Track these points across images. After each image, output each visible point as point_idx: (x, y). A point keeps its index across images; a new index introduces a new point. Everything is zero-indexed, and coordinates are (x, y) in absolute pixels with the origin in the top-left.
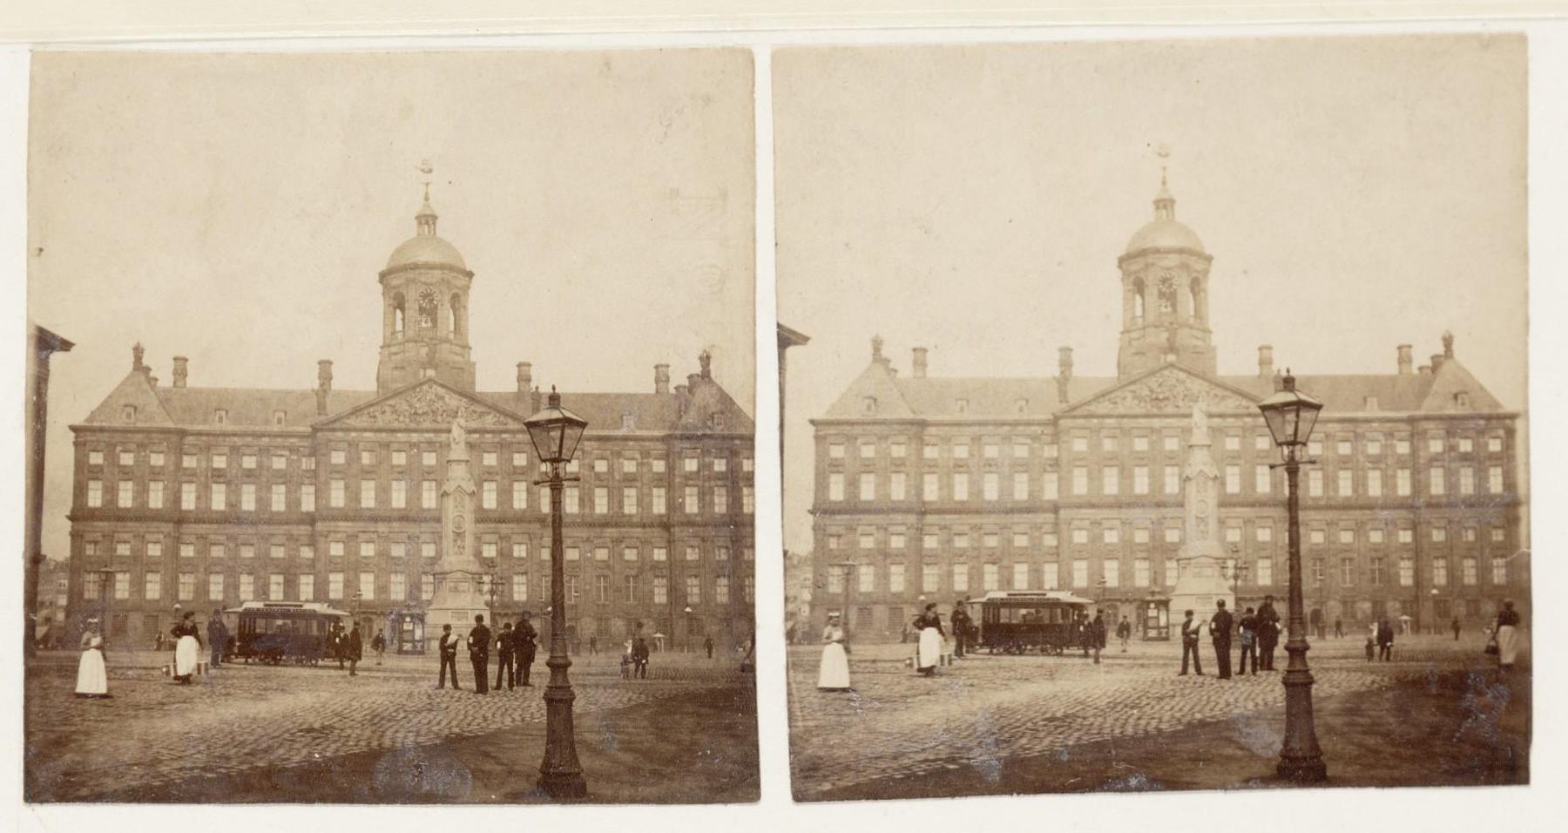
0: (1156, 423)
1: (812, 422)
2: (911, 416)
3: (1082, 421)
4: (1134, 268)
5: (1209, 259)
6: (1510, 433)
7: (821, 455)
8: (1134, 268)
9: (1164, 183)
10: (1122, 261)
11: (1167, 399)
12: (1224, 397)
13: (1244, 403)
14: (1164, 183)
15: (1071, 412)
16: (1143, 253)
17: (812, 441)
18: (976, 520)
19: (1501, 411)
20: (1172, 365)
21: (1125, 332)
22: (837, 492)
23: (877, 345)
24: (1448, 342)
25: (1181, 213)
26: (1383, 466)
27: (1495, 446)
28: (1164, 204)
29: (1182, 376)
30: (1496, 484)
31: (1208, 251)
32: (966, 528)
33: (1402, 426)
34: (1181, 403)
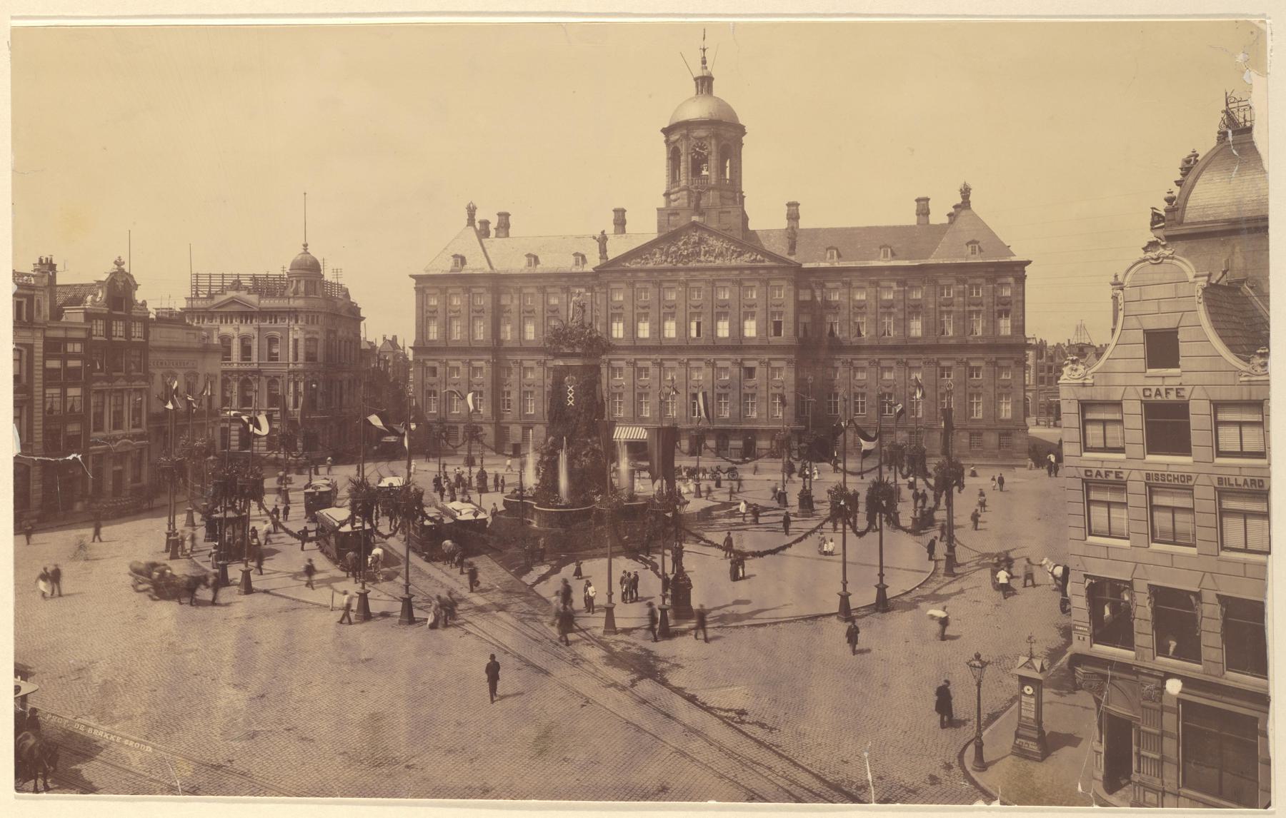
2: (488, 270)
6: (1021, 279)
8: (674, 137)
9: (704, 62)
10: (667, 131)
14: (704, 62)
17: (414, 292)
19: (1013, 259)
21: (667, 195)
23: (472, 211)
24: (966, 192)
25: (717, 91)
26: (895, 310)
27: (1007, 292)
28: (705, 83)
30: (1005, 327)
31: (741, 122)
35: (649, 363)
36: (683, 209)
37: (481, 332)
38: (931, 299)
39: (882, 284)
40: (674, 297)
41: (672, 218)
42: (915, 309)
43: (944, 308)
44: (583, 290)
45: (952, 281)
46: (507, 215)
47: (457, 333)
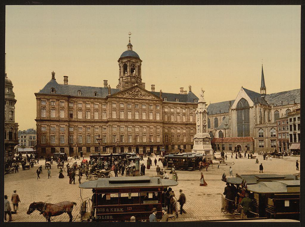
0: (133, 101)
1: (36, 94)
3: (115, 99)
4: (124, 61)
5: (141, 61)
7: (39, 105)
9: (130, 41)
11: (136, 95)
12: (149, 96)
13: (154, 97)
14: (130, 41)
15: (111, 97)
16: (127, 57)
18: (85, 124)
20: (137, 86)
22: (44, 115)
29: (140, 90)
32: (81, 126)
33: (184, 106)
34: (139, 96)
35: (124, 126)
36: (130, 82)
37: (63, 115)
38: (188, 112)
39: (178, 108)
40: (131, 107)
41: (126, 84)
42: (184, 114)
43: (191, 115)
44: (98, 104)
45: (193, 108)
46: (68, 77)
47: (54, 115)
